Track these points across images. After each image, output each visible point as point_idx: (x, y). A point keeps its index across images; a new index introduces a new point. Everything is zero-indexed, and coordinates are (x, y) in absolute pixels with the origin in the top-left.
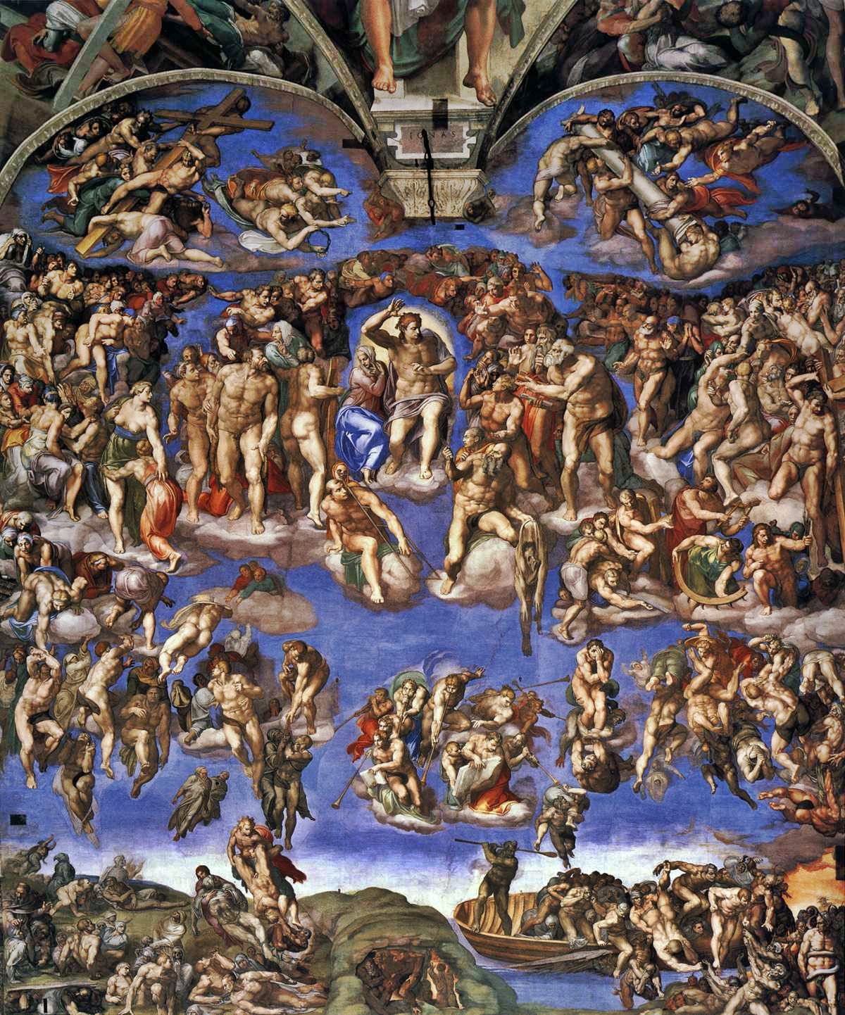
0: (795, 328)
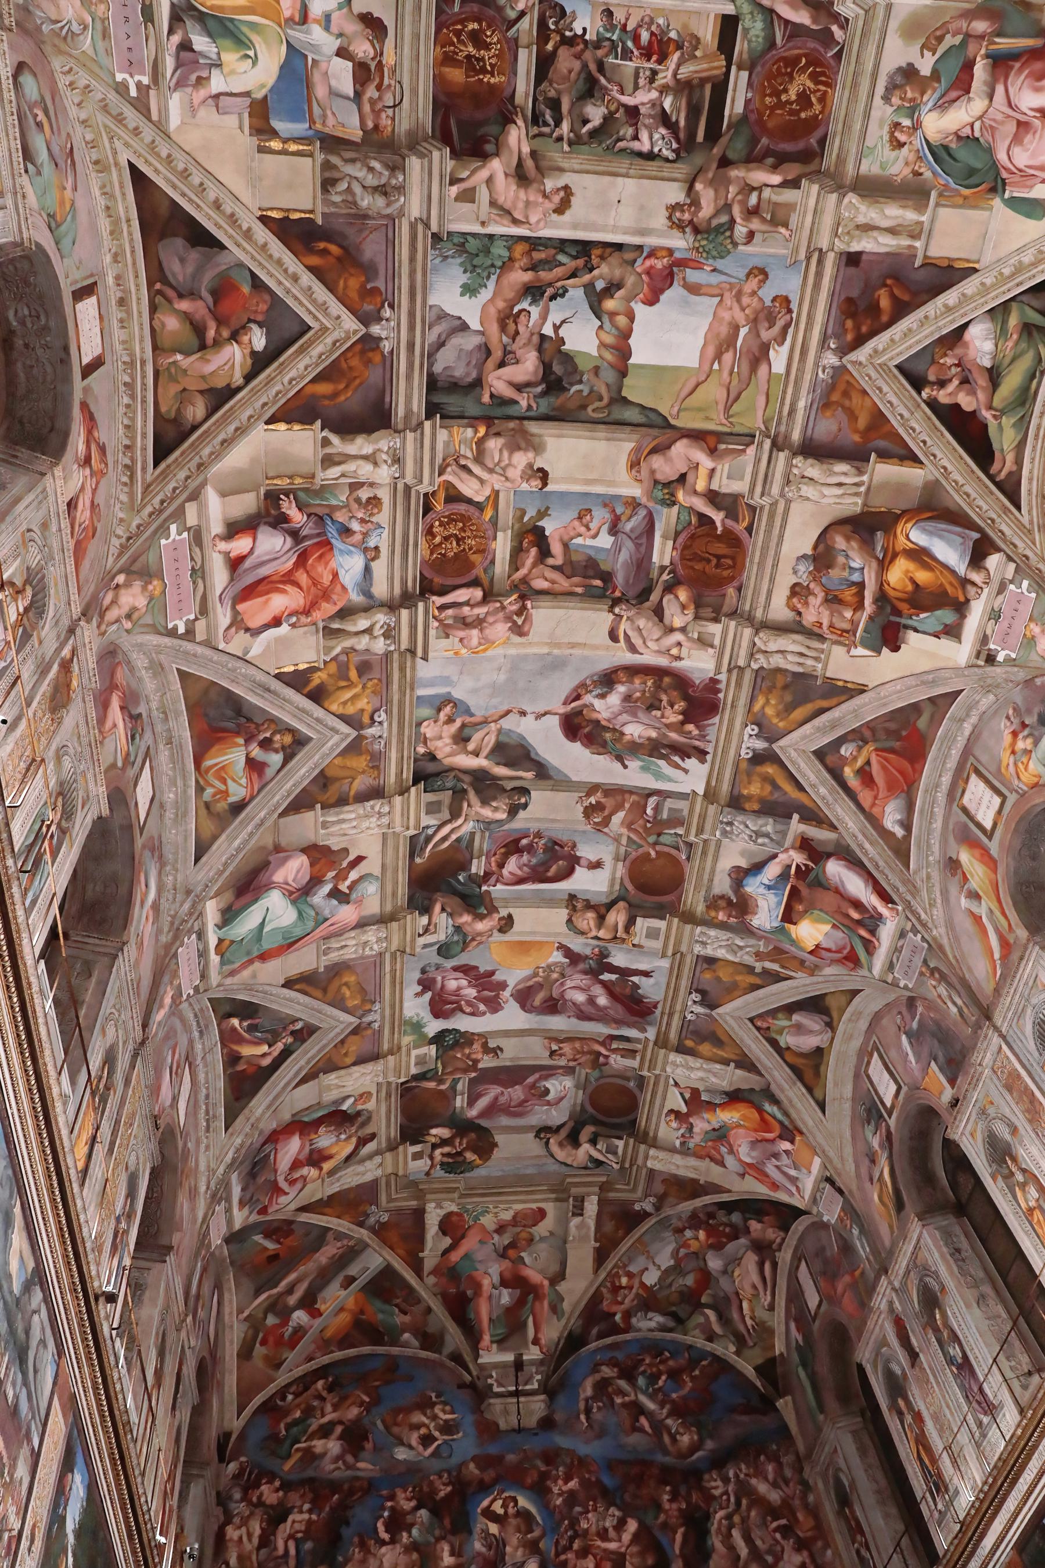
0: (762, 1488)
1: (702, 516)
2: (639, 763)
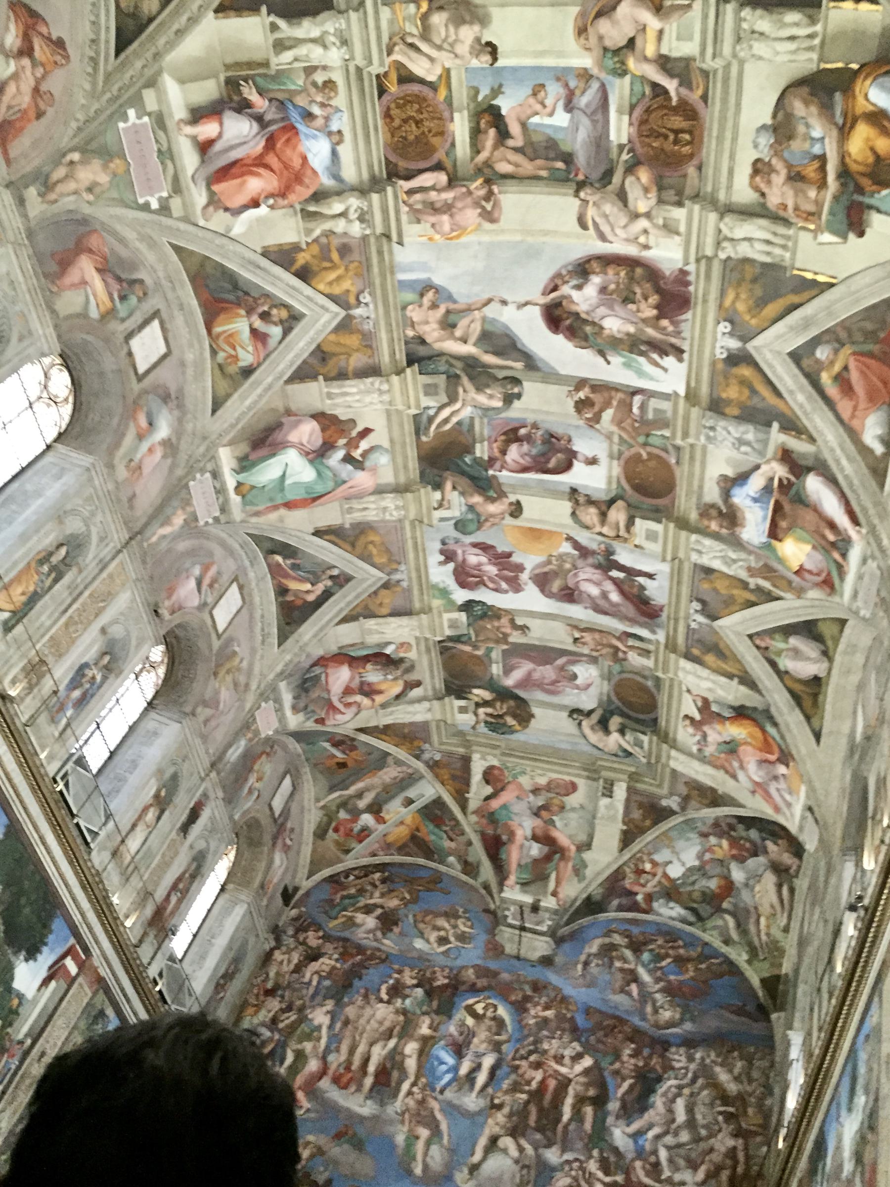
0: (723, 1077)
1: (655, 86)
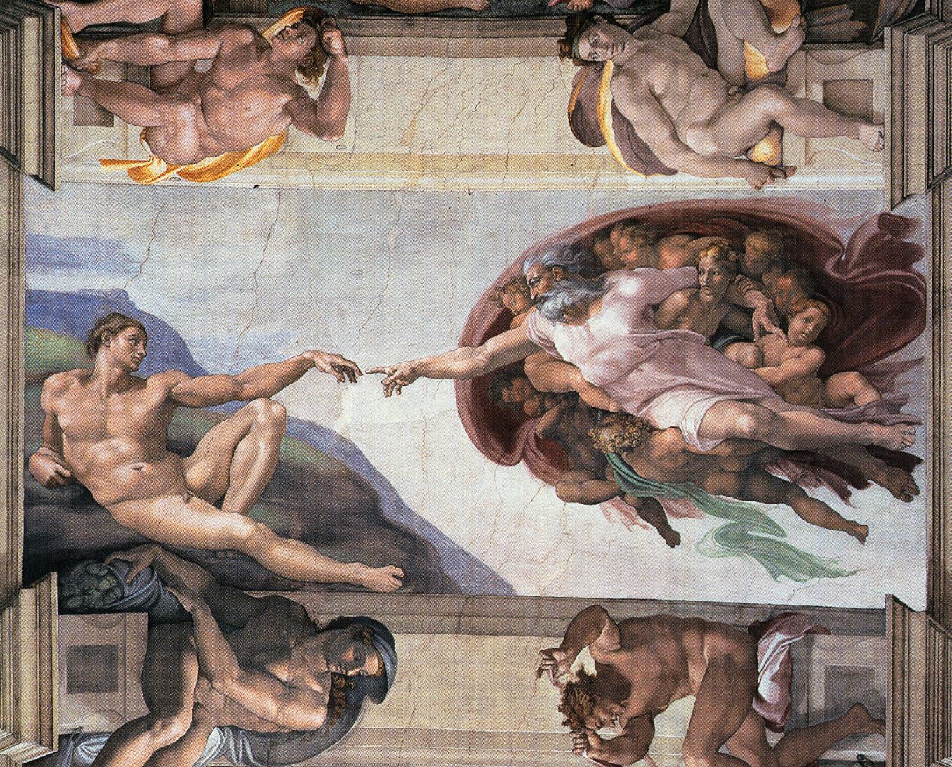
2: (714, 523)
